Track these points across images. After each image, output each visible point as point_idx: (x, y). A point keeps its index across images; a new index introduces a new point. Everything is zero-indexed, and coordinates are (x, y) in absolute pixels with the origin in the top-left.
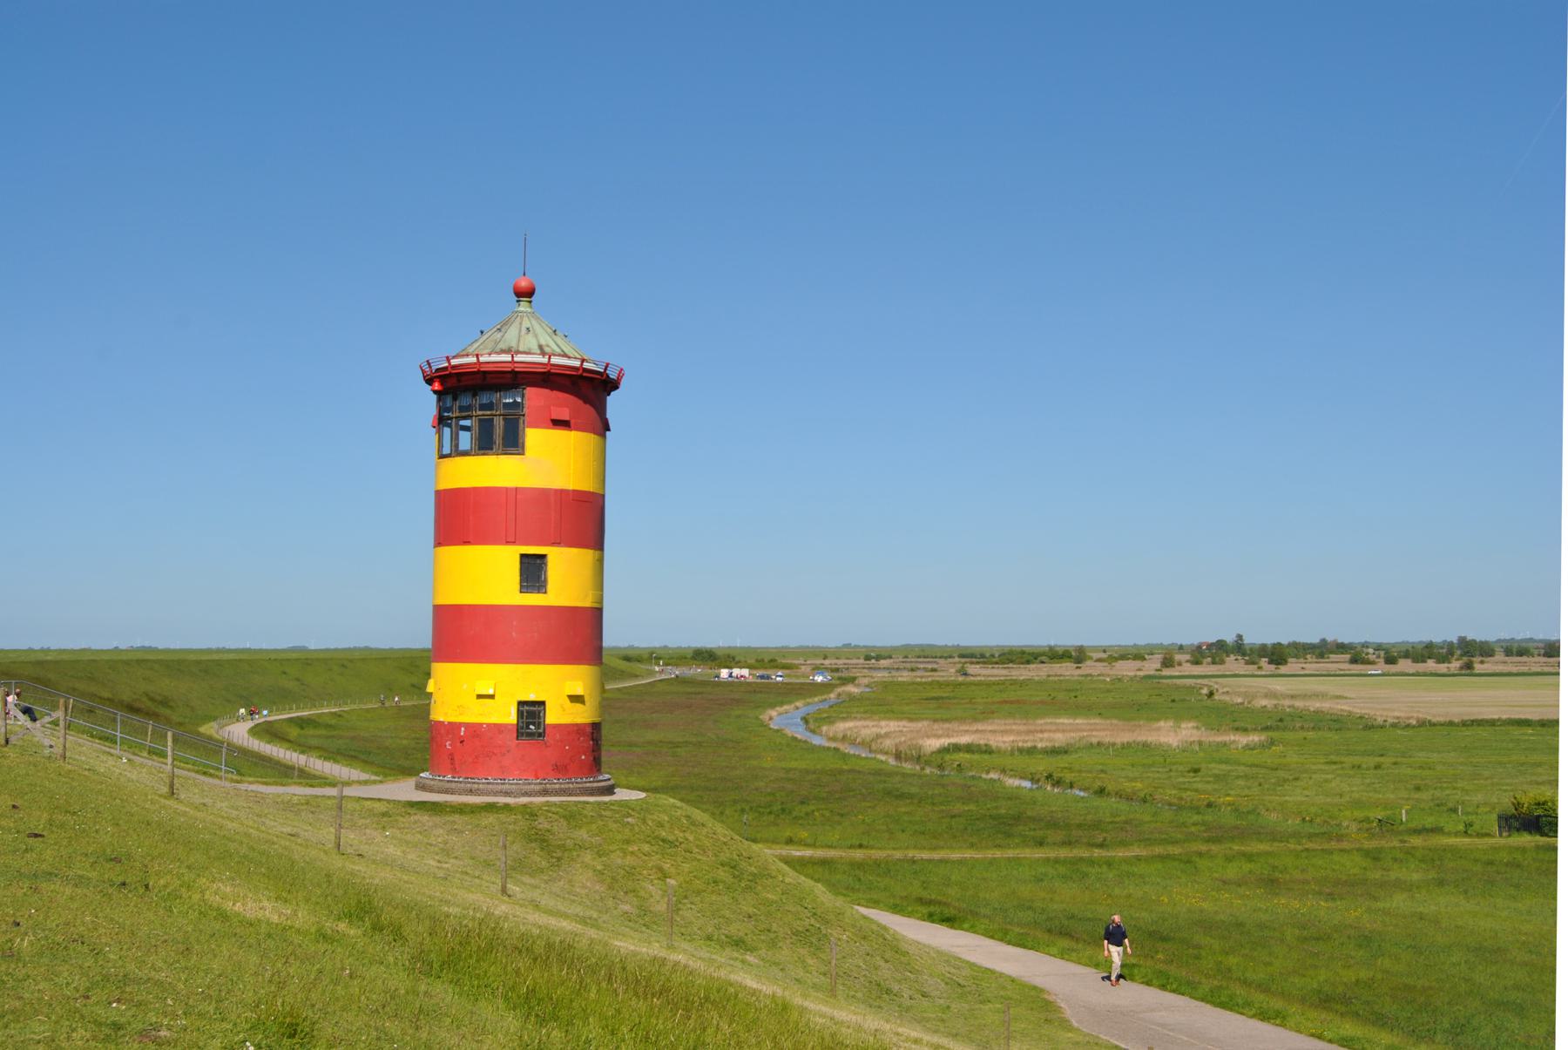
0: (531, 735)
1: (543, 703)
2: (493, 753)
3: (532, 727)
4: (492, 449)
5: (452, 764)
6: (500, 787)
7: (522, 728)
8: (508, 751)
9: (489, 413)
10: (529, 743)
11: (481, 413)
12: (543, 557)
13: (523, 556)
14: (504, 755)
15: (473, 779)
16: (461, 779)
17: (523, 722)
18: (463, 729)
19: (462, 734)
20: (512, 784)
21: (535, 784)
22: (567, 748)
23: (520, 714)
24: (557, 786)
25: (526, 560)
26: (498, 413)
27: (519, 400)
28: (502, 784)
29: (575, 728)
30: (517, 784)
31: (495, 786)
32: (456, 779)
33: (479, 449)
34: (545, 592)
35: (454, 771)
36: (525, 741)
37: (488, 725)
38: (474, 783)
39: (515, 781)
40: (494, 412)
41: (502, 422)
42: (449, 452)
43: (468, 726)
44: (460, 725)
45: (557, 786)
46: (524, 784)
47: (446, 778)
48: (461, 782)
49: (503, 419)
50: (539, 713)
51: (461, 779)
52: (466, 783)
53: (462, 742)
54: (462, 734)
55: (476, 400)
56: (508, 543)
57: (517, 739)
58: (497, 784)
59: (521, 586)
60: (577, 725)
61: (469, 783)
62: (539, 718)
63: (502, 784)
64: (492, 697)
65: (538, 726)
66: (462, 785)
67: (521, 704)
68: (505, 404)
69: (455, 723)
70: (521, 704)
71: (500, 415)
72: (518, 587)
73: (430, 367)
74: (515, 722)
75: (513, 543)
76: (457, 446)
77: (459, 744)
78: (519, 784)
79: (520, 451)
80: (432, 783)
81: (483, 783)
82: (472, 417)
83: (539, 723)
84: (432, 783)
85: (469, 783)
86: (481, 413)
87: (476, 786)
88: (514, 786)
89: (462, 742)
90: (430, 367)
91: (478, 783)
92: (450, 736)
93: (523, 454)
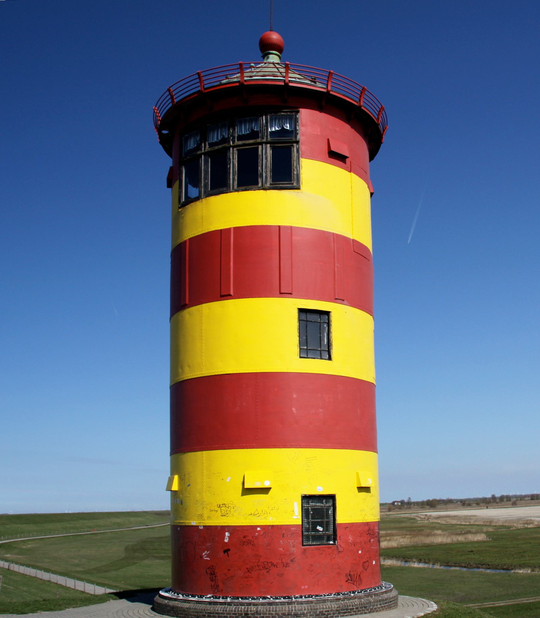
0: (318, 538)
1: (332, 498)
2: (273, 564)
3: (319, 528)
4: (258, 184)
5: (212, 580)
7: (308, 530)
8: (292, 561)
9: (251, 141)
10: (319, 549)
11: (240, 143)
13: (301, 311)
14: (287, 565)
15: (246, 598)
16: (229, 600)
17: (308, 523)
18: (227, 534)
19: (226, 541)
20: (301, 603)
21: (331, 601)
22: (360, 552)
23: (305, 512)
24: (357, 601)
25: (304, 317)
26: (265, 140)
27: (287, 127)
28: (289, 603)
29: (367, 528)
30: (308, 602)
31: (279, 608)
32: (221, 600)
33: (239, 185)
34: (330, 358)
35: (217, 591)
36: (313, 548)
37: (263, 527)
38: (250, 604)
39: (304, 599)
40: (259, 140)
41: (269, 152)
42: (197, 195)
43: (234, 530)
44: (223, 529)
45: (357, 601)
46: (318, 602)
47: (204, 599)
48: (229, 604)
49: (273, 148)
50: (328, 510)
51: (229, 600)
52: (237, 604)
53: (226, 551)
54: (226, 541)
55: (234, 129)
56: (282, 294)
57: (303, 545)
59: (300, 349)
60: (367, 524)
61: (242, 604)
62: (328, 516)
65: (326, 527)
66: (233, 608)
68: (272, 133)
69: (216, 527)
70: (306, 498)
71: (266, 143)
72: (297, 350)
73: (172, 98)
74: (300, 523)
75: (289, 294)
77: (221, 554)
78: (311, 602)
79: (295, 184)
80: (186, 605)
81: (263, 604)
82: (229, 148)
83: (328, 523)
84: (186, 605)
85: (242, 604)
86: (240, 143)
87: (253, 608)
89: (226, 551)
90: (172, 98)
91: (255, 605)
92: (209, 544)
93: (298, 188)
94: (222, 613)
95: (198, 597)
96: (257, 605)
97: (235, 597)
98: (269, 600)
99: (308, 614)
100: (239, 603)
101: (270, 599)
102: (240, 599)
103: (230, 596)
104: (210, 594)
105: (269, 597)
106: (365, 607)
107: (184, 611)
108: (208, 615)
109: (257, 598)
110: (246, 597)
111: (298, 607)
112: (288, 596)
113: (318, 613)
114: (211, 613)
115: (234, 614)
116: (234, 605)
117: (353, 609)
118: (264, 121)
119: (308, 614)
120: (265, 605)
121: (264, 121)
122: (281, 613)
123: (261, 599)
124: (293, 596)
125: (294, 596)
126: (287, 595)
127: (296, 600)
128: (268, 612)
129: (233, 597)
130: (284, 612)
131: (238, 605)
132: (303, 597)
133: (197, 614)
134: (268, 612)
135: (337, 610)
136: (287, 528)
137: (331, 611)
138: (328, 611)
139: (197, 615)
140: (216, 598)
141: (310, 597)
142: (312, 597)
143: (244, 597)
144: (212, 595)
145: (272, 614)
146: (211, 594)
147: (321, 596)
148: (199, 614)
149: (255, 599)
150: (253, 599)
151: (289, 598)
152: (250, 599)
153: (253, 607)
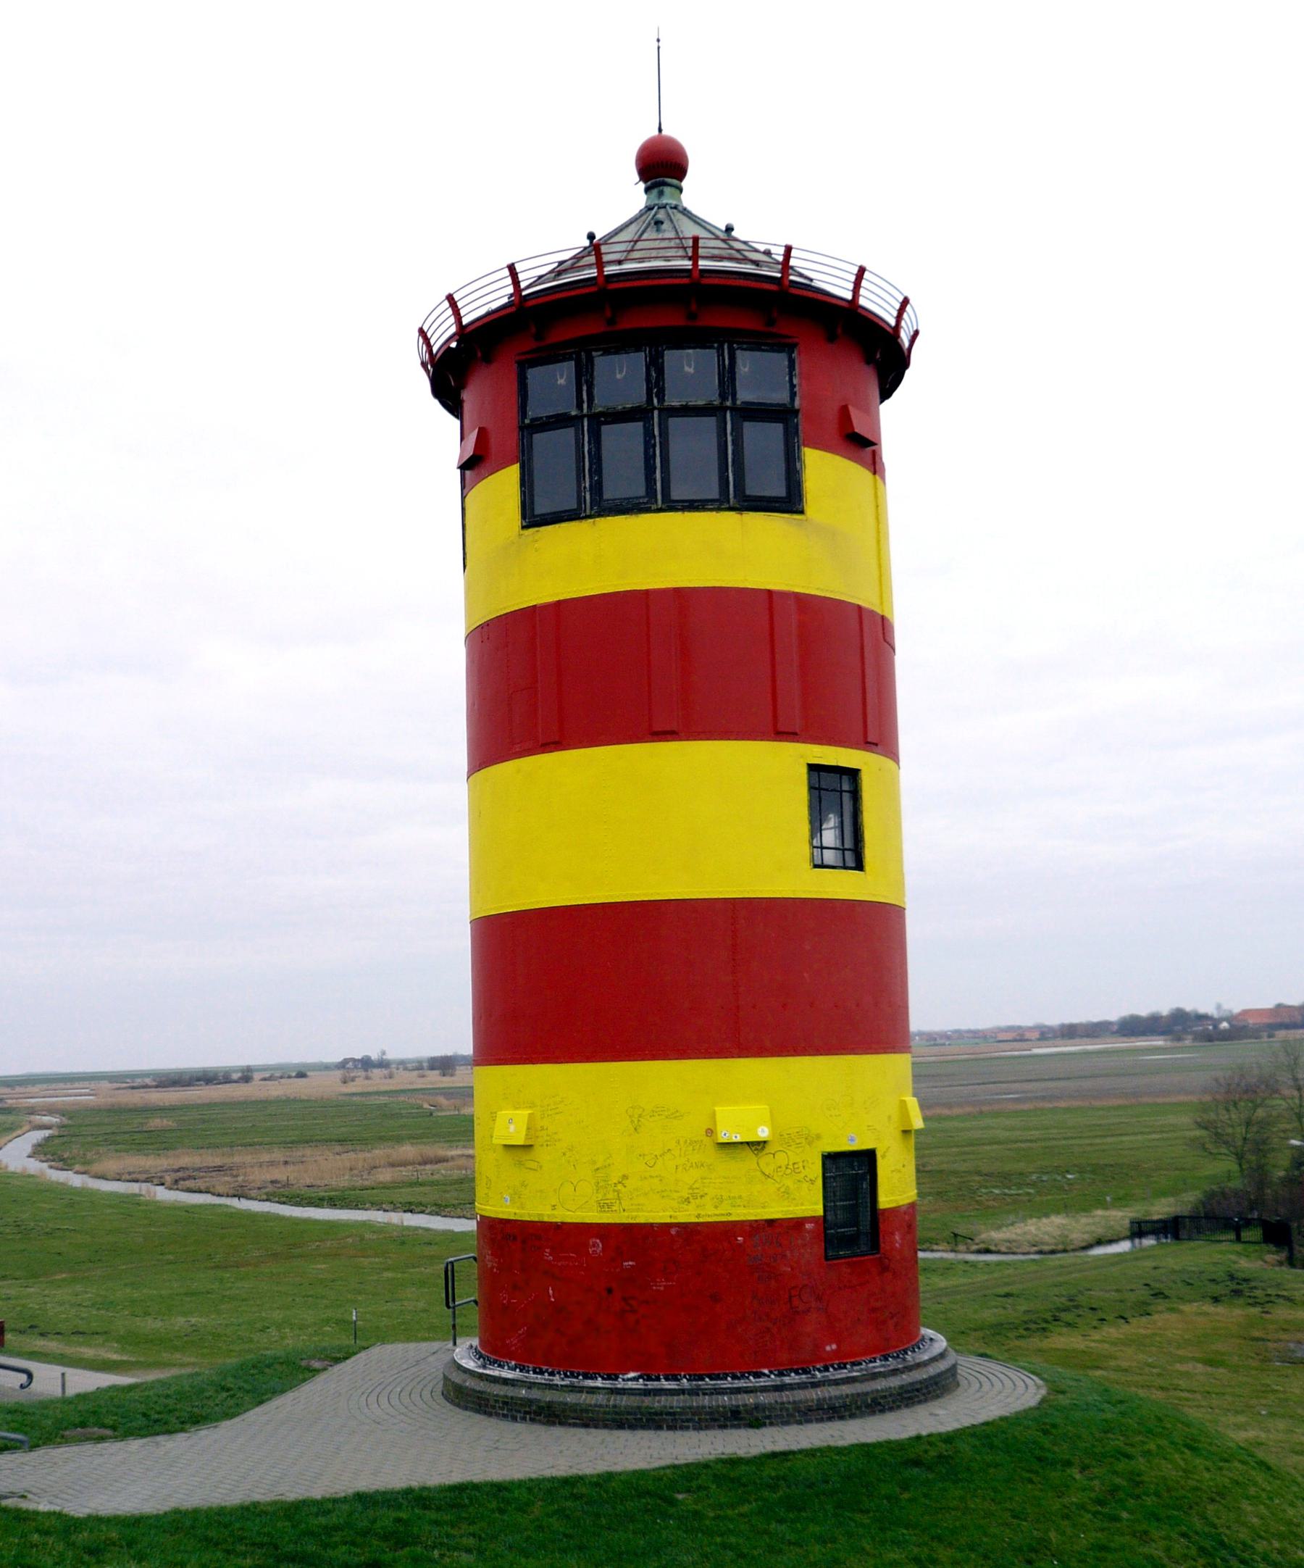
1: (869, 1158)
6: (800, 1395)
12: (853, 774)
15: (718, 1377)
47: (620, 1384)
52: (694, 1392)
58: (791, 1387)
63: (801, 1386)
64: (758, 1146)
67: (831, 1160)
70: (831, 1160)
73: (516, 282)
76: (597, 488)
88: (846, 1389)
90: (516, 282)
93: (802, 512)
94: (681, 1414)
95: (603, 1379)
96: (752, 1392)
97: (695, 1375)
98: (766, 1379)
99: (854, 1406)
100: (715, 1389)
101: (769, 1376)
102: (707, 1380)
103: (683, 1374)
104: (634, 1371)
105: (766, 1371)
106: (936, 1384)
107: (587, 1411)
108: (646, 1419)
109: (743, 1376)
110: (719, 1374)
111: (833, 1391)
112: (803, 1369)
113: (869, 1401)
114: (656, 1414)
115: (707, 1413)
116: (705, 1394)
117: (921, 1389)
118: (727, 362)
119: (854, 1406)
120: (769, 1391)
121: (727, 362)
122: (805, 1407)
123: (751, 1378)
124: (811, 1368)
125: (814, 1367)
126: (800, 1366)
127: (823, 1377)
128: (778, 1407)
129: (690, 1375)
130: (810, 1404)
131: (712, 1394)
132: (831, 1369)
133: (617, 1417)
134: (778, 1407)
135: (899, 1394)
136: (797, 1224)
137: (890, 1395)
138: (885, 1397)
139: (621, 1419)
140: (649, 1379)
141: (842, 1368)
142: (845, 1368)
143: (714, 1374)
144: (639, 1373)
145: (787, 1409)
146: (637, 1371)
147: (861, 1364)
148: (626, 1416)
149: (739, 1378)
150: (734, 1377)
151: (805, 1372)
152: (729, 1379)
153: (746, 1396)
